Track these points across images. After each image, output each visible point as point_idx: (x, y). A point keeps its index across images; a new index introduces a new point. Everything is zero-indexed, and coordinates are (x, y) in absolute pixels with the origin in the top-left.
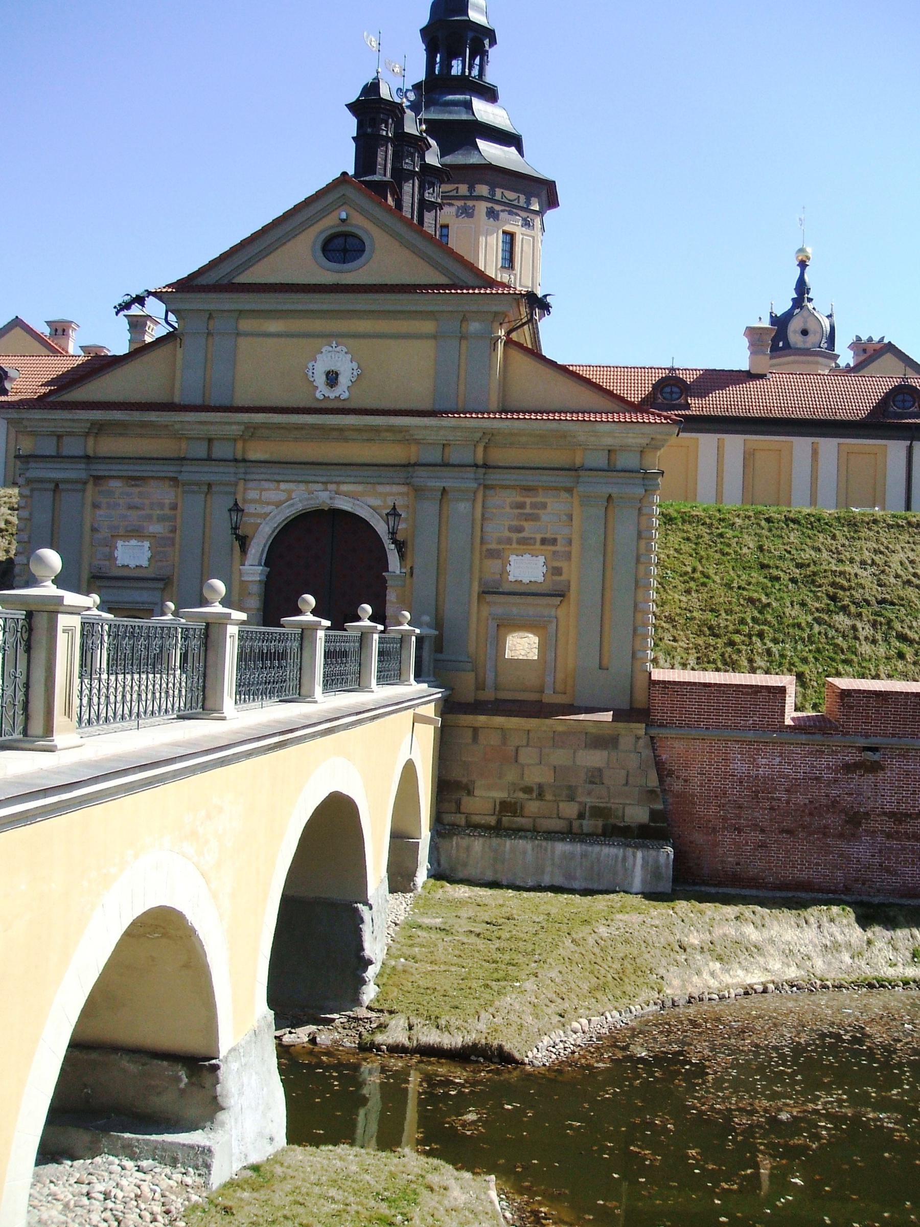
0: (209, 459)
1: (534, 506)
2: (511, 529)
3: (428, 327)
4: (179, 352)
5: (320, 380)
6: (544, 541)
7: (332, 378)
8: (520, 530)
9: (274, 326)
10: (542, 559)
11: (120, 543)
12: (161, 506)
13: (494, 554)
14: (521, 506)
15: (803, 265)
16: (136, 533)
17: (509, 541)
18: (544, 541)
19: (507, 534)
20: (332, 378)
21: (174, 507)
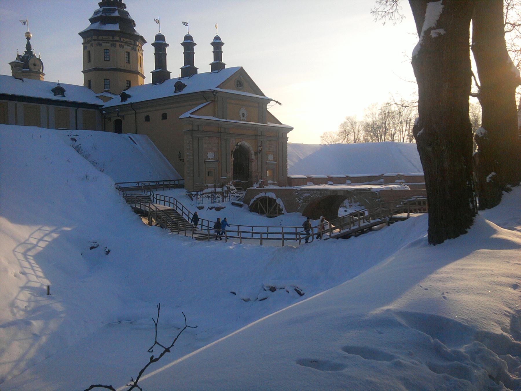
5: (241, 116)
6: (273, 152)
7: (243, 114)
15: (28, 38)
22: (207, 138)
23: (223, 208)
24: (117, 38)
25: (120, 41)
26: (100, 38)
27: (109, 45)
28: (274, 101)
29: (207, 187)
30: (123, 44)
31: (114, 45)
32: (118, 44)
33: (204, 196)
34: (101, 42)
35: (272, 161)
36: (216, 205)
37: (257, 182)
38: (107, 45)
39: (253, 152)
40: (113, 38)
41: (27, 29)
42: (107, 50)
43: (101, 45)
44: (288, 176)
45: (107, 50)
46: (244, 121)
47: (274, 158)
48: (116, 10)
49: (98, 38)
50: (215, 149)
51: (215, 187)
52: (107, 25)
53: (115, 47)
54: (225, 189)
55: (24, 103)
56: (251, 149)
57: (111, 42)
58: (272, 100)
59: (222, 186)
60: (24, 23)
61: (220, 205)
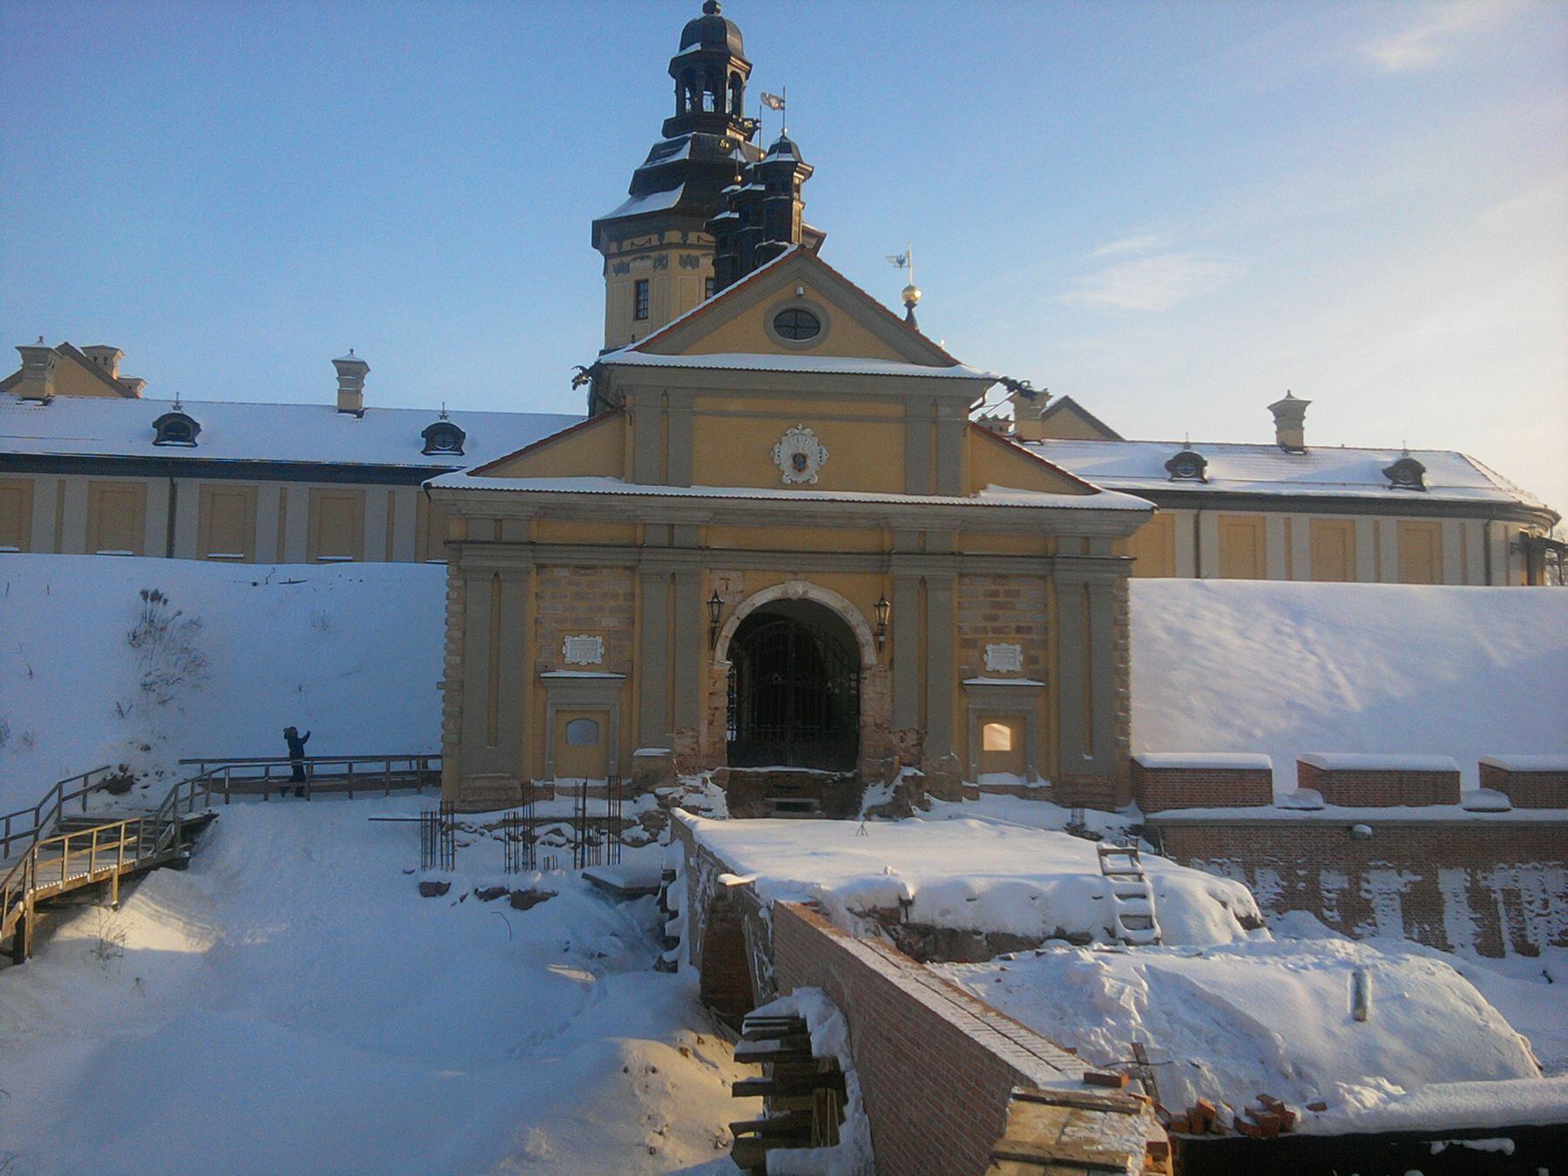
0: (671, 546)
1: (1007, 593)
2: (986, 618)
3: (896, 410)
4: (629, 430)
5: (787, 465)
6: (1019, 630)
7: (799, 461)
8: (995, 618)
9: (734, 405)
10: (1018, 648)
11: (568, 639)
12: (615, 596)
13: (968, 644)
14: (995, 594)
16: (584, 626)
17: (985, 631)
18: (1019, 630)
19: (982, 624)
20: (799, 461)
21: (631, 596)
22: (564, 573)
23: (545, 897)
24: (674, 236)
25: (684, 245)
26: (626, 245)
27: (649, 263)
28: (1004, 381)
29: (549, 793)
30: (693, 253)
31: (662, 263)
32: (674, 255)
33: (538, 831)
34: (626, 259)
35: (1010, 674)
36: (515, 882)
37: (886, 777)
38: (641, 268)
39: (864, 634)
40: (661, 236)
41: (909, 276)
42: (641, 286)
43: (623, 269)
44: (1135, 753)
45: (641, 286)
46: (807, 486)
47: (1030, 660)
48: (685, 141)
49: (620, 246)
50: (610, 622)
51: (584, 792)
52: (651, 197)
53: (665, 266)
54: (648, 803)
55: (312, 484)
56: (854, 618)
57: (655, 254)
58: (994, 381)
59: (613, 793)
60: (901, 262)
61: (536, 879)
